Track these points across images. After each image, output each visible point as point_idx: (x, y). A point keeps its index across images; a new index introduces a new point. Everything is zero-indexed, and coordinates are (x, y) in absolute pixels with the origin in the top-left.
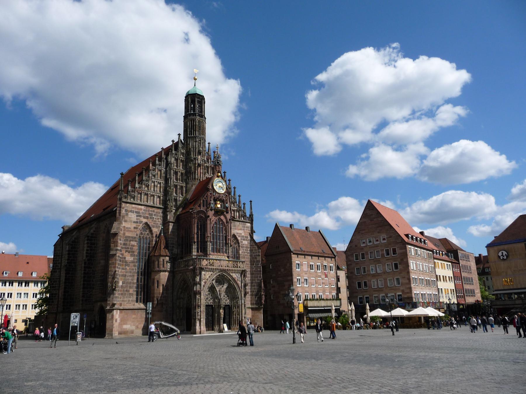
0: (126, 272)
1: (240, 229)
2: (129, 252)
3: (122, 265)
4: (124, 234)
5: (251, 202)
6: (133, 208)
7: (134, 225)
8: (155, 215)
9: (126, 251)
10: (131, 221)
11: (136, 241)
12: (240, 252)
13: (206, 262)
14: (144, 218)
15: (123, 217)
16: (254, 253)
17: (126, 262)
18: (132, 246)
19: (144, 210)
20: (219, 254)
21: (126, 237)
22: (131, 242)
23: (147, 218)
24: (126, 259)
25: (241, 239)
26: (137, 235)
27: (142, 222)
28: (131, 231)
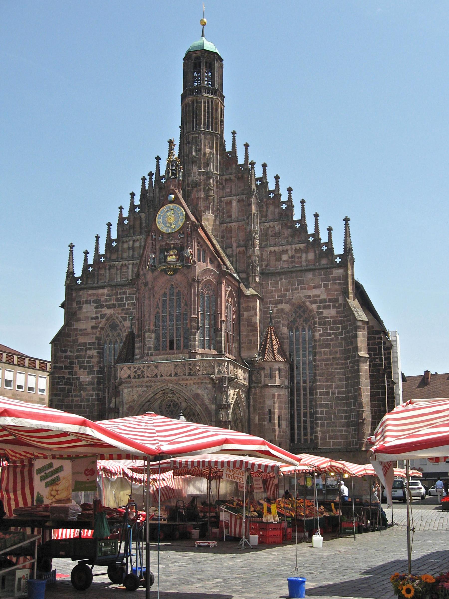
0: (81, 402)
1: (315, 287)
2: (85, 368)
3: (75, 390)
4: (76, 341)
5: (346, 220)
6: (90, 295)
7: (93, 323)
8: (127, 299)
9: (81, 367)
10: (87, 318)
11: (95, 349)
12: (317, 335)
13: (128, 372)
14: (109, 307)
15: (75, 314)
16: (348, 332)
17: (81, 384)
18: (89, 357)
19: (108, 295)
20: (171, 351)
21: (80, 345)
22: (88, 351)
23: (114, 306)
24: (81, 380)
25: (319, 307)
26: (97, 338)
27: (106, 314)
28: (87, 334)
